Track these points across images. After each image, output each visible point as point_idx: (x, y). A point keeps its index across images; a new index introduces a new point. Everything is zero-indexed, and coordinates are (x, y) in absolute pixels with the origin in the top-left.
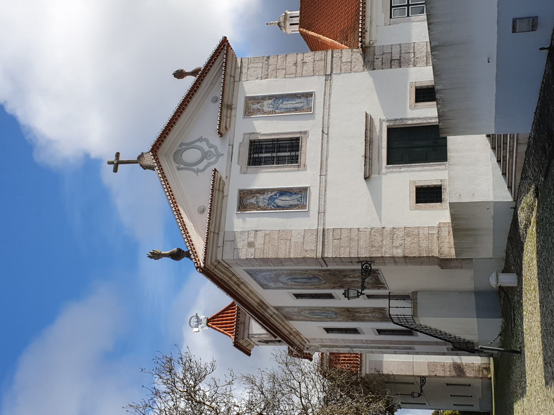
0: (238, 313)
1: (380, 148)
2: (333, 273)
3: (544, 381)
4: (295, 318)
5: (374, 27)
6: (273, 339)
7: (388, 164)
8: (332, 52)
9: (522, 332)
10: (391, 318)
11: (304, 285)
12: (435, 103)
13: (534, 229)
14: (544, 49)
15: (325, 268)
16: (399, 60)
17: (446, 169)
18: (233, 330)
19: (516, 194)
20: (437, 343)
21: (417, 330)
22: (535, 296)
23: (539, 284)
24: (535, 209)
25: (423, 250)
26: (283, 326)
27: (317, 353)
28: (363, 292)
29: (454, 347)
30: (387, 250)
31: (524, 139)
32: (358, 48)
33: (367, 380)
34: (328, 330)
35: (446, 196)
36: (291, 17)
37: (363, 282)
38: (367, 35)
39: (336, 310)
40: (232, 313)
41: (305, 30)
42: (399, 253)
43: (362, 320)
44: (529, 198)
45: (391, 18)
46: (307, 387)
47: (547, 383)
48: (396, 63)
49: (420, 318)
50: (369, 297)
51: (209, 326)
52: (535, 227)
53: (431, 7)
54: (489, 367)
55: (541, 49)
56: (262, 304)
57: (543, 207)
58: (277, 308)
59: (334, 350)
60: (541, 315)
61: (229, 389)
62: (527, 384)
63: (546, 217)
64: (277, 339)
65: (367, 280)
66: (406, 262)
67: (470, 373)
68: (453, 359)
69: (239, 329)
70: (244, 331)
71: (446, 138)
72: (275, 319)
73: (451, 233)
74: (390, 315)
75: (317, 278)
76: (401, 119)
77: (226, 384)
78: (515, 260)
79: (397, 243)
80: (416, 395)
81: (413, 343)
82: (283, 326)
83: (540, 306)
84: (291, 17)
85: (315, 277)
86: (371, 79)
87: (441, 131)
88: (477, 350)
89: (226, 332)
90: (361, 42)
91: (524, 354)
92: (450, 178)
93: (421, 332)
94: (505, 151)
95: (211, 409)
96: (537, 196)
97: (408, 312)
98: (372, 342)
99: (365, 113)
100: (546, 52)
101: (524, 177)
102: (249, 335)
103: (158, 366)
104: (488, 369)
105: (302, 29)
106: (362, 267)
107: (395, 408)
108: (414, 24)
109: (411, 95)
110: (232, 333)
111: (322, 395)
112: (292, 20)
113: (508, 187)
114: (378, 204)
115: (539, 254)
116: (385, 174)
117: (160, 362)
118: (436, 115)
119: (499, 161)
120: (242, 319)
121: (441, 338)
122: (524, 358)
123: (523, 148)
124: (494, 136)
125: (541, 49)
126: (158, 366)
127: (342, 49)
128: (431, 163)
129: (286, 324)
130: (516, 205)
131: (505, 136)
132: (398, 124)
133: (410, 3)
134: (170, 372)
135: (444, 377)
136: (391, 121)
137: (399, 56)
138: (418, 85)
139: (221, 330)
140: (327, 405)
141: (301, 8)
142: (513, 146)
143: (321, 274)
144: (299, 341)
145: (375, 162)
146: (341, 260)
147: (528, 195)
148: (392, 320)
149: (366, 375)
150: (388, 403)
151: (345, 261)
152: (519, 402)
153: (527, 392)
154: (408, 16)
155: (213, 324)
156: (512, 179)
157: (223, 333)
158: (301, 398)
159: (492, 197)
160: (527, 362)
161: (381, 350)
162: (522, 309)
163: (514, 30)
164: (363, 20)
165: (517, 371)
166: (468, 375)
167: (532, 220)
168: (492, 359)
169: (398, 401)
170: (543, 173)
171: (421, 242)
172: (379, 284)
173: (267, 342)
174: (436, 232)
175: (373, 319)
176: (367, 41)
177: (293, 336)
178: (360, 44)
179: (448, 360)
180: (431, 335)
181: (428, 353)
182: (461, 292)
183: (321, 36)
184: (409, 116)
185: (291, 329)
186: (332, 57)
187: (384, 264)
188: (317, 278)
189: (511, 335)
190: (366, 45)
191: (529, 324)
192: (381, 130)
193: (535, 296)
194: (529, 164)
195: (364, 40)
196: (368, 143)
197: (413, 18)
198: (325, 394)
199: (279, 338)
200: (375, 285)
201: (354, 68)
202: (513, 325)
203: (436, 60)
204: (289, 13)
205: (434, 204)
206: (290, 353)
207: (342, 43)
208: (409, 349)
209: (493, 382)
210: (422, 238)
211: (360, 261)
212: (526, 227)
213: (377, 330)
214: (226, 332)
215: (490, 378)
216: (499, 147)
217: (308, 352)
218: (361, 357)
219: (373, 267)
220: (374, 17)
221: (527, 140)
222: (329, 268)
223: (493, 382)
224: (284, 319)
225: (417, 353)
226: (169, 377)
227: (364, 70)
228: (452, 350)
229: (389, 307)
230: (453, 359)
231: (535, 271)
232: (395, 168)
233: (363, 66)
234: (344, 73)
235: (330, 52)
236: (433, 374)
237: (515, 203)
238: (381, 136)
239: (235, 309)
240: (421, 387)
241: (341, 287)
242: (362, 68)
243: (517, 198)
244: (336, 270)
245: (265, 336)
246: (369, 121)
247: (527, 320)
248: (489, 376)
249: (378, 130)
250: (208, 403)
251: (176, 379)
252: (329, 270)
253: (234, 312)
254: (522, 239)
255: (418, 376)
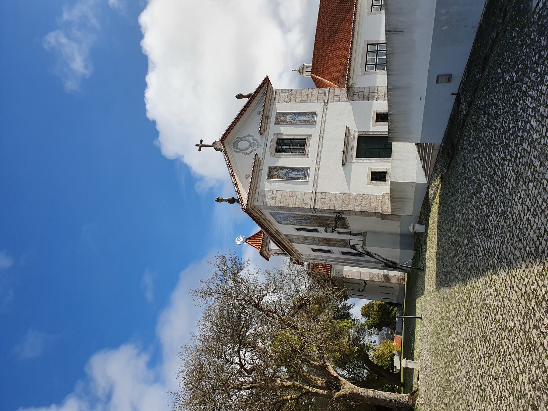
0: (264, 237)
1: (352, 148)
2: (319, 218)
3: (435, 286)
4: (295, 241)
5: (355, 76)
6: (282, 252)
7: (356, 157)
8: (329, 89)
9: (425, 259)
10: (350, 245)
11: (301, 224)
12: (387, 123)
13: (438, 199)
14: (454, 94)
15: (315, 214)
16: (368, 96)
17: (390, 162)
18: (260, 245)
19: (429, 179)
20: (376, 262)
21: (364, 254)
22: (434, 238)
23: (438, 231)
24: (440, 188)
25: (372, 208)
26: (288, 246)
27: (306, 263)
28: (336, 230)
29: (385, 265)
30: (352, 207)
31: (437, 147)
32: (345, 87)
33: (333, 279)
34: (314, 250)
35: (388, 178)
36: (306, 67)
37: (336, 224)
38: (351, 80)
39: (319, 239)
40: (260, 236)
41: (314, 75)
42: (358, 209)
43: (333, 246)
44: (437, 182)
45: (365, 71)
46: (300, 280)
47: (437, 288)
48: (366, 98)
49: (367, 247)
50: (339, 233)
51: (247, 242)
52: (439, 198)
53: (390, 65)
54: (404, 278)
55: (452, 94)
56: (277, 232)
57: (444, 187)
58: (286, 235)
59: (317, 262)
60: (437, 249)
61: (256, 277)
62: (425, 288)
63: (446, 193)
64: (284, 253)
65: (338, 223)
66: (362, 215)
67: (393, 281)
68: (384, 272)
69: (263, 246)
70: (266, 247)
71: (391, 144)
72: (284, 241)
73: (390, 199)
74: (350, 244)
75: (310, 220)
76: (367, 131)
77: (255, 273)
78: (425, 217)
79: (358, 203)
80: (361, 290)
81: (362, 261)
82: (288, 246)
83: (437, 244)
84: (306, 67)
85: (308, 219)
86: (351, 106)
87: (389, 139)
88: (399, 268)
89: (256, 247)
90: (346, 84)
91: (425, 271)
92: (391, 167)
93: (367, 255)
94: (425, 153)
95: (245, 287)
96: (441, 181)
97: (361, 243)
98: (338, 258)
99: (345, 127)
100: (455, 96)
101: (435, 169)
102: (269, 249)
103: (218, 261)
104: (403, 279)
105: (312, 75)
106: (336, 215)
107: (348, 297)
108: (379, 75)
109: (373, 117)
110: (259, 247)
111: (307, 285)
112: (307, 69)
113: (425, 175)
114: (348, 181)
115: (439, 214)
116: (355, 163)
117: (219, 258)
118: (387, 130)
119: (421, 159)
120: (265, 240)
121: (378, 259)
122: (425, 273)
123: (436, 152)
124: (420, 144)
125: (452, 94)
126: (218, 261)
127: (335, 87)
128: (382, 158)
129: (290, 244)
130: (429, 186)
131: (426, 144)
132: (364, 134)
133: (377, 63)
134: (224, 264)
135: (378, 282)
136: (360, 132)
137: (368, 94)
138: (378, 112)
139: (253, 245)
140: (310, 291)
141: (313, 62)
142: (430, 151)
143: (312, 218)
144: (296, 254)
145: (349, 155)
146: (324, 211)
147: (436, 180)
148: (351, 247)
149: (333, 277)
150: (344, 292)
151: (327, 211)
152: (420, 298)
153: (425, 292)
154: (376, 70)
155: (249, 242)
156: (428, 171)
157: (254, 247)
158: (296, 285)
159: (415, 180)
160: (427, 275)
161: (343, 264)
162: (427, 245)
163: (437, 82)
164: (349, 71)
165: (420, 280)
166: (392, 282)
167: (437, 194)
168: (406, 273)
169: (350, 292)
170: (446, 168)
171: (371, 203)
172: (345, 226)
173: (279, 254)
174: (381, 198)
175: (340, 245)
176: (350, 84)
177: (294, 252)
178: (346, 85)
179: (381, 272)
180: (372, 257)
181: (370, 268)
182: (392, 234)
183: (324, 79)
184: (371, 130)
185: (293, 248)
186: (329, 92)
187: (349, 215)
188: (310, 220)
189: (419, 260)
190: (350, 86)
191: (430, 254)
192: (354, 137)
193: (434, 238)
194: (439, 162)
195: (348, 83)
196: (346, 144)
197: (378, 72)
198: (309, 285)
199: (286, 252)
200: (342, 226)
201: (341, 99)
202: (420, 254)
203: (390, 97)
204: (305, 64)
205: (381, 182)
206: (291, 260)
207: (335, 84)
208: (359, 264)
209: (405, 287)
210: (372, 201)
211: (335, 212)
212: (433, 198)
213: (342, 252)
214: (256, 247)
215: (404, 285)
216: (422, 151)
217: (301, 261)
218: (331, 267)
219: (343, 216)
220: (356, 69)
221: (439, 148)
222: (317, 214)
223: (405, 287)
224: (289, 241)
225: (364, 267)
226: (223, 267)
227: (347, 101)
228: (384, 266)
229: (350, 239)
230: (384, 272)
231: (436, 224)
232: (360, 160)
233: (347, 99)
234: (335, 102)
235: (328, 89)
236: (371, 280)
237: (428, 184)
238: (354, 141)
239: (262, 234)
240: (364, 286)
241: (323, 226)
242: (346, 100)
243: (430, 182)
244: (321, 216)
245: (278, 250)
246: (348, 131)
247: (429, 252)
248: (404, 283)
249: (352, 137)
250: (244, 283)
251: (227, 268)
252: (317, 216)
253: (261, 236)
254: (430, 205)
255: (363, 280)
